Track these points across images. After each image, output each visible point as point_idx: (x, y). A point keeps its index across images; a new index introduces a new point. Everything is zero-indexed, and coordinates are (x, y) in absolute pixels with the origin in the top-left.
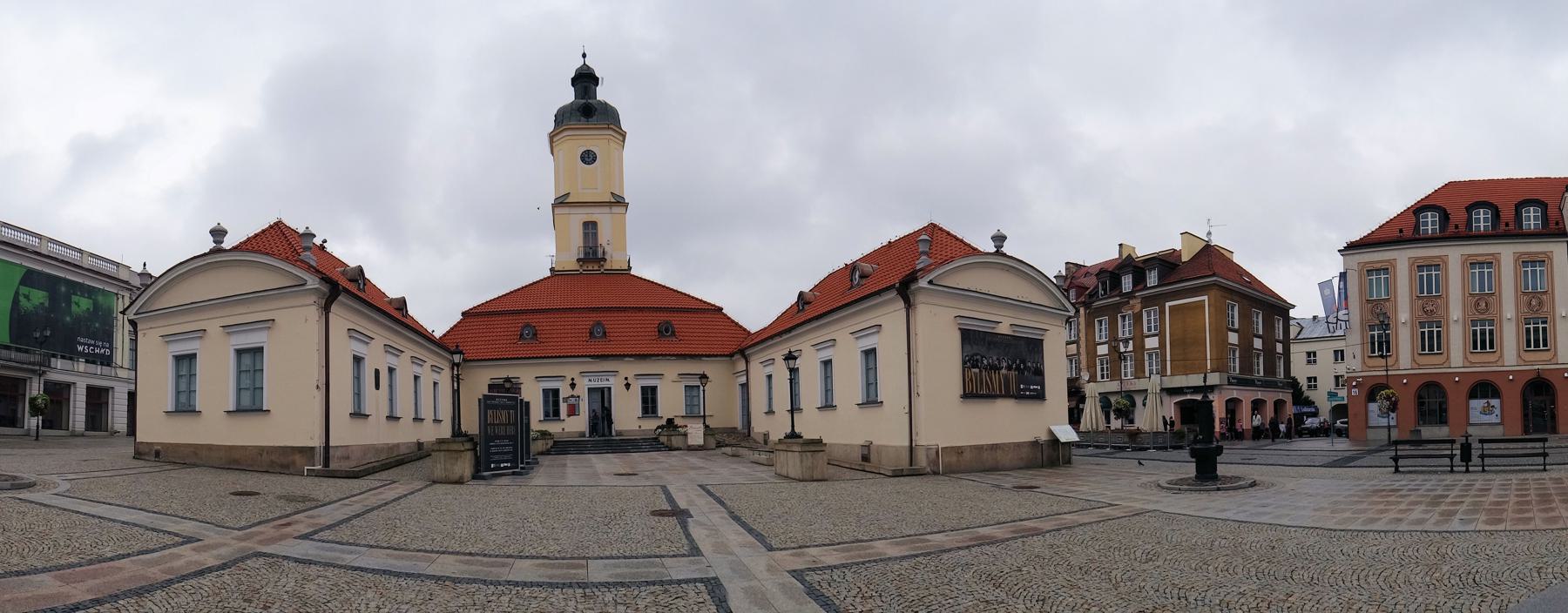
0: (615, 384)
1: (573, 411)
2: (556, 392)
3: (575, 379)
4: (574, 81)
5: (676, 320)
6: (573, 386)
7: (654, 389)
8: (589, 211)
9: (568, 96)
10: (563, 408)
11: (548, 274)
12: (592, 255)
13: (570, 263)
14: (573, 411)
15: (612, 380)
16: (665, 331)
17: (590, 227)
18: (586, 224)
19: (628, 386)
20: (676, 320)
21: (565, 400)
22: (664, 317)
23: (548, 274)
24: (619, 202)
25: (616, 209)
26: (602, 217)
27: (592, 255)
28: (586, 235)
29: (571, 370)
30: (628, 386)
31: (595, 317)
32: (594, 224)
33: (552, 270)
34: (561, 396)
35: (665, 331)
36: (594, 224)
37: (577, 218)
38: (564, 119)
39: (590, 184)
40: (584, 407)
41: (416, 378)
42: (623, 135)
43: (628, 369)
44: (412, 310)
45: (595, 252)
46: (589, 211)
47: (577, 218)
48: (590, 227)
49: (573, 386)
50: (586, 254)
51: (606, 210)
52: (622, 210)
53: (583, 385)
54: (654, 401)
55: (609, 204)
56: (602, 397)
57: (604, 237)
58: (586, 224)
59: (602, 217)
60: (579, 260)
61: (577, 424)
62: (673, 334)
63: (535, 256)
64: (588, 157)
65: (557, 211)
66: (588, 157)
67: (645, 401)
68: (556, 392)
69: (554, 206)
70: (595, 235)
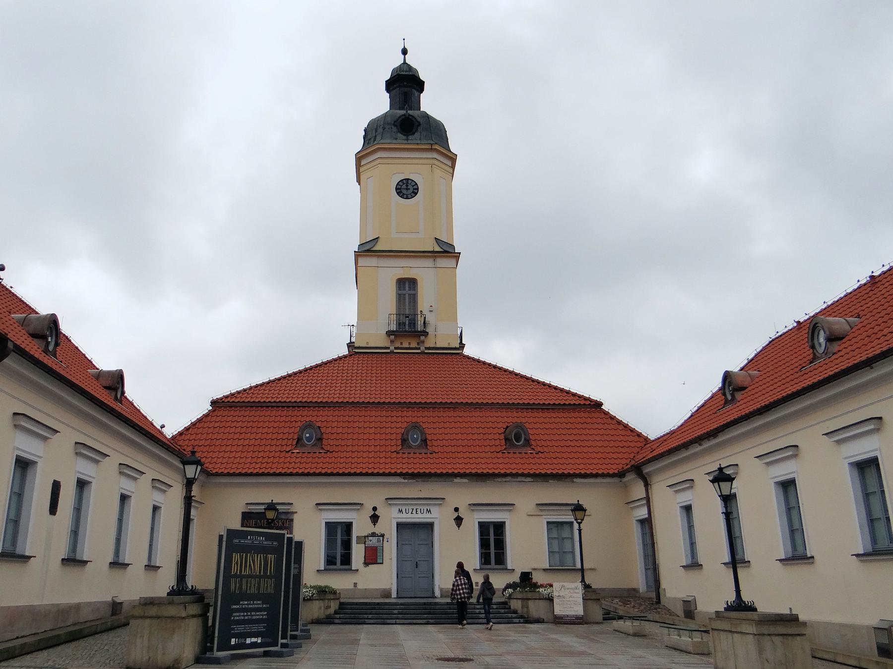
0: (440, 517)
1: (373, 557)
3: (378, 508)
4: (390, 85)
5: (533, 423)
6: (375, 518)
7: (499, 527)
8: (407, 265)
10: (358, 553)
11: (345, 352)
12: (409, 326)
13: (377, 338)
14: (373, 557)
15: (434, 510)
16: (515, 438)
17: (407, 287)
19: (459, 521)
20: (533, 423)
21: (362, 540)
23: (345, 352)
24: (446, 251)
25: (442, 262)
26: (425, 274)
27: (409, 326)
28: (400, 298)
29: (372, 495)
30: (459, 521)
31: (412, 416)
32: (413, 282)
33: (350, 345)
34: (355, 533)
35: (515, 438)
36: (413, 282)
37: (388, 274)
38: (374, 133)
39: (408, 227)
40: (390, 550)
41: (124, 498)
42: (453, 159)
43: (461, 495)
44: (131, 391)
45: (413, 323)
46: (407, 265)
47: (388, 274)
48: (407, 287)
49: (375, 518)
50: (400, 324)
51: (428, 262)
52: (450, 262)
53: (391, 518)
54: (500, 544)
55: (433, 255)
56: (417, 533)
57: (426, 300)
59: (425, 274)
60: (389, 333)
61: (377, 579)
62: (528, 442)
63: (326, 322)
64: (407, 189)
65: (362, 261)
66: (407, 189)
67: (484, 544)
69: (358, 255)
70: (414, 298)
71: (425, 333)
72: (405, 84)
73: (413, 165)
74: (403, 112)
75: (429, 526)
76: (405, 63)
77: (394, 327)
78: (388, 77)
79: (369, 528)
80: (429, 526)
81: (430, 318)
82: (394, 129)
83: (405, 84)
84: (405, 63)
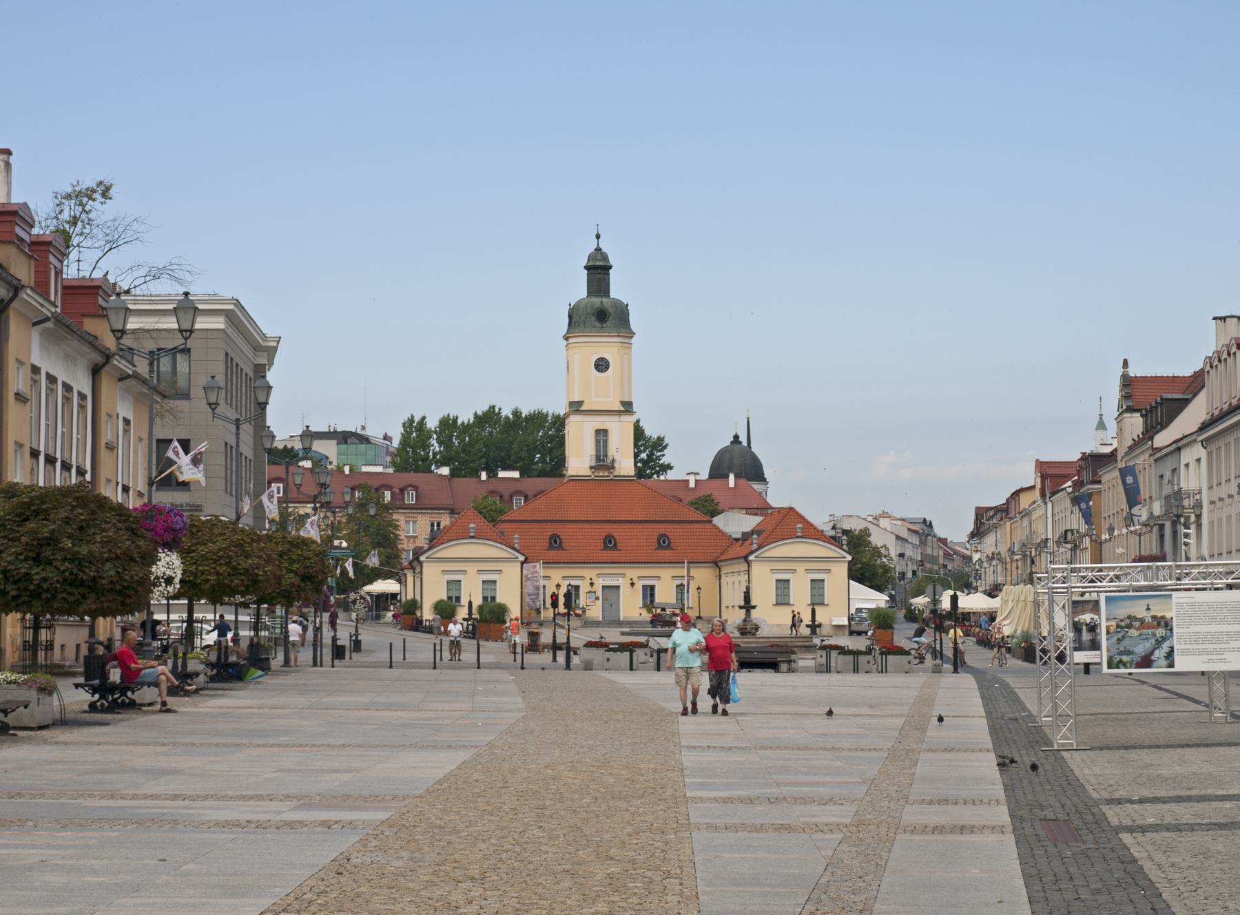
0: (622, 582)
2: (577, 588)
4: (586, 267)
6: (592, 584)
7: (652, 588)
9: (578, 290)
18: (598, 432)
19: (632, 584)
22: (662, 528)
28: (597, 442)
29: (589, 573)
30: (632, 584)
32: (605, 432)
36: (605, 432)
42: (631, 334)
43: (633, 573)
48: (602, 435)
49: (592, 584)
50: (598, 458)
51: (616, 418)
53: (600, 583)
54: (652, 595)
55: (619, 413)
58: (598, 432)
60: (591, 468)
66: (602, 365)
68: (577, 588)
70: (606, 442)
71: (613, 468)
72: (598, 271)
73: (607, 347)
74: (596, 301)
75: (618, 587)
76: (598, 249)
77: (594, 464)
78: (585, 263)
79: (589, 589)
80: (618, 587)
81: (617, 457)
82: (593, 318)
83: (598, 271)
84: (598, 249)
